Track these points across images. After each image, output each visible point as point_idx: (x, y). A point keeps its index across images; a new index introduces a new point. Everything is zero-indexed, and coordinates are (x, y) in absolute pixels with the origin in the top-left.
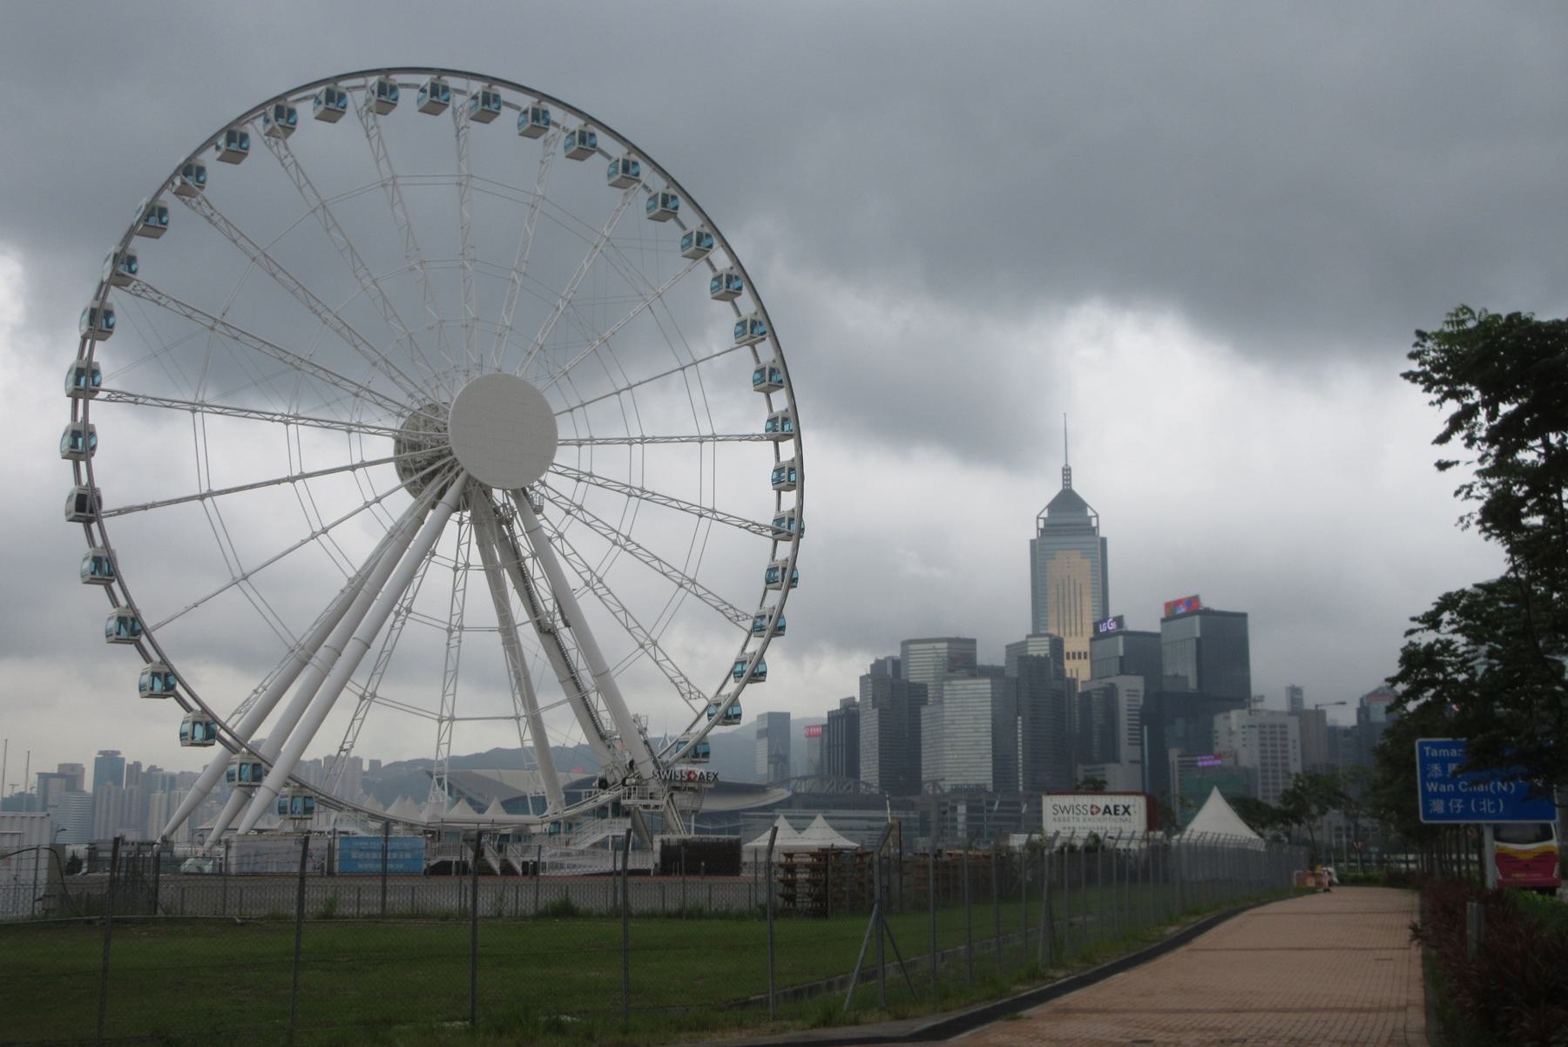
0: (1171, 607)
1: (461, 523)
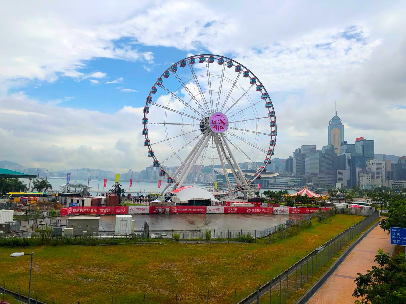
0: (357, 139)
1: (212, 139)
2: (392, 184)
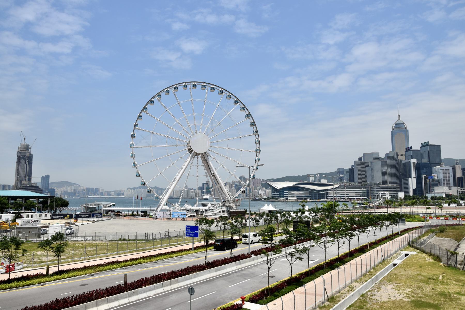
2: (459, 191)
